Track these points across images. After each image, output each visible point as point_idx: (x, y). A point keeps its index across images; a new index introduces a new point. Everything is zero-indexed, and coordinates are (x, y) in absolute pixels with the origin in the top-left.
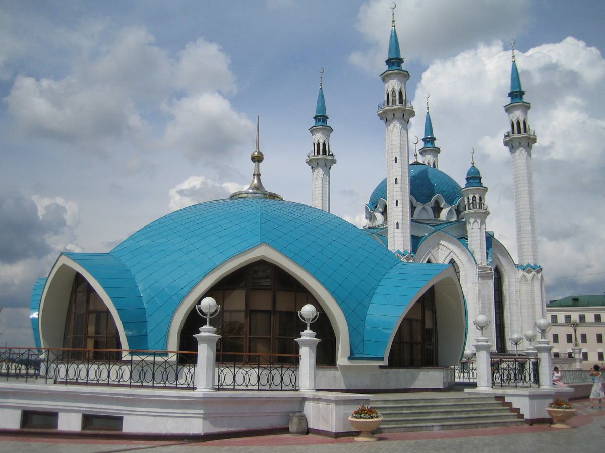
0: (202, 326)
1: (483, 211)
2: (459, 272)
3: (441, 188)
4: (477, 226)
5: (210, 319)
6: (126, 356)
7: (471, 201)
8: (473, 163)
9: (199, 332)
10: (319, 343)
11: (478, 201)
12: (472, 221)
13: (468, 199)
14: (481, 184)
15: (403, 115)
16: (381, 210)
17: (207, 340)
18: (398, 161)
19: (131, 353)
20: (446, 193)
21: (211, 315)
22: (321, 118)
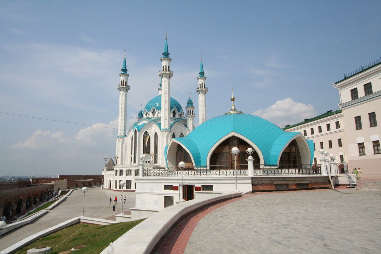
4: (191, 121)
5: (251, 154)
6: (261, 167)
11: (192, 112)
14: (192, 106)
16: (152, 112)
22: (125, 70)
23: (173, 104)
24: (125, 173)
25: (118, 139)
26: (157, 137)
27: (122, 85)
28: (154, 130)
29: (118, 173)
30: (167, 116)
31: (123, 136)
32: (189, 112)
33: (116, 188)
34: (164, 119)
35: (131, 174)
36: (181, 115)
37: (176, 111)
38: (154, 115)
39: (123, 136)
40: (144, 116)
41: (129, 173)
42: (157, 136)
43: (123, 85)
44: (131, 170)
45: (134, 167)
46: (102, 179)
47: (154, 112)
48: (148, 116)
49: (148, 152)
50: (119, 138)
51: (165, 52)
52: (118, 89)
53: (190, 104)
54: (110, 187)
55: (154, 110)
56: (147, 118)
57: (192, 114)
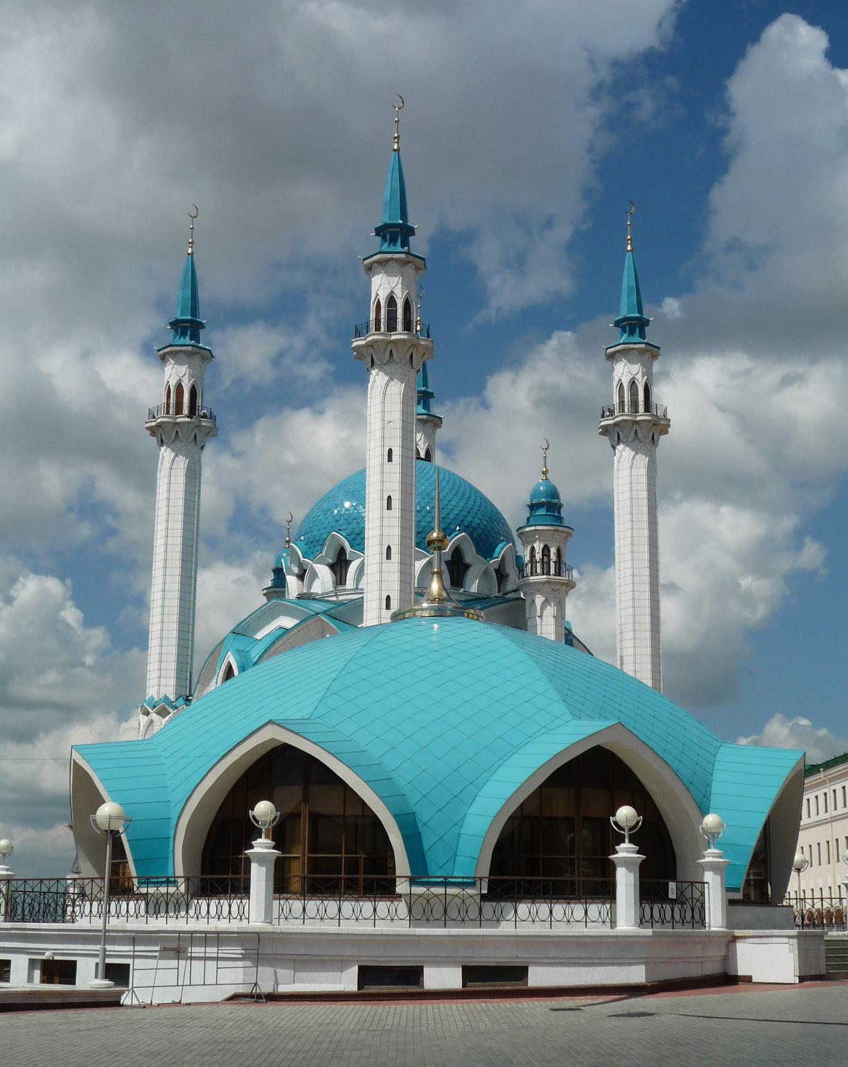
0: (620, 845)
1: (563, 578)
3: (469, 519)
6: (402, 887)
7: (538, 556)
8: (545, 473)
9: (616, 852)
10: (643, 861)
11: (553, 557)
12: (539, 600)
13: (533, 548)
14: (559, 519)
15: (411, 357)
17: (627, 863)
18: (394, 457)
19: (413, 881)
20: (479, 531)
21: (630, 830)
23: (452, 516)
27: (171, 410)
30: (396, 586)
31: (172, 698)
36: (501, 575)
37: (470, 555)
38: (340, 579)
39: (172, 698)
40: (291, 581)
43: (179, 410)
47: (339, 565)
48: (310, 587)
50: (147, 713)
51: (386, 219)
52: (153, 431)
53: (542, 512)
55: (342, 551)
56: (301, 597)
57: (558, 573)
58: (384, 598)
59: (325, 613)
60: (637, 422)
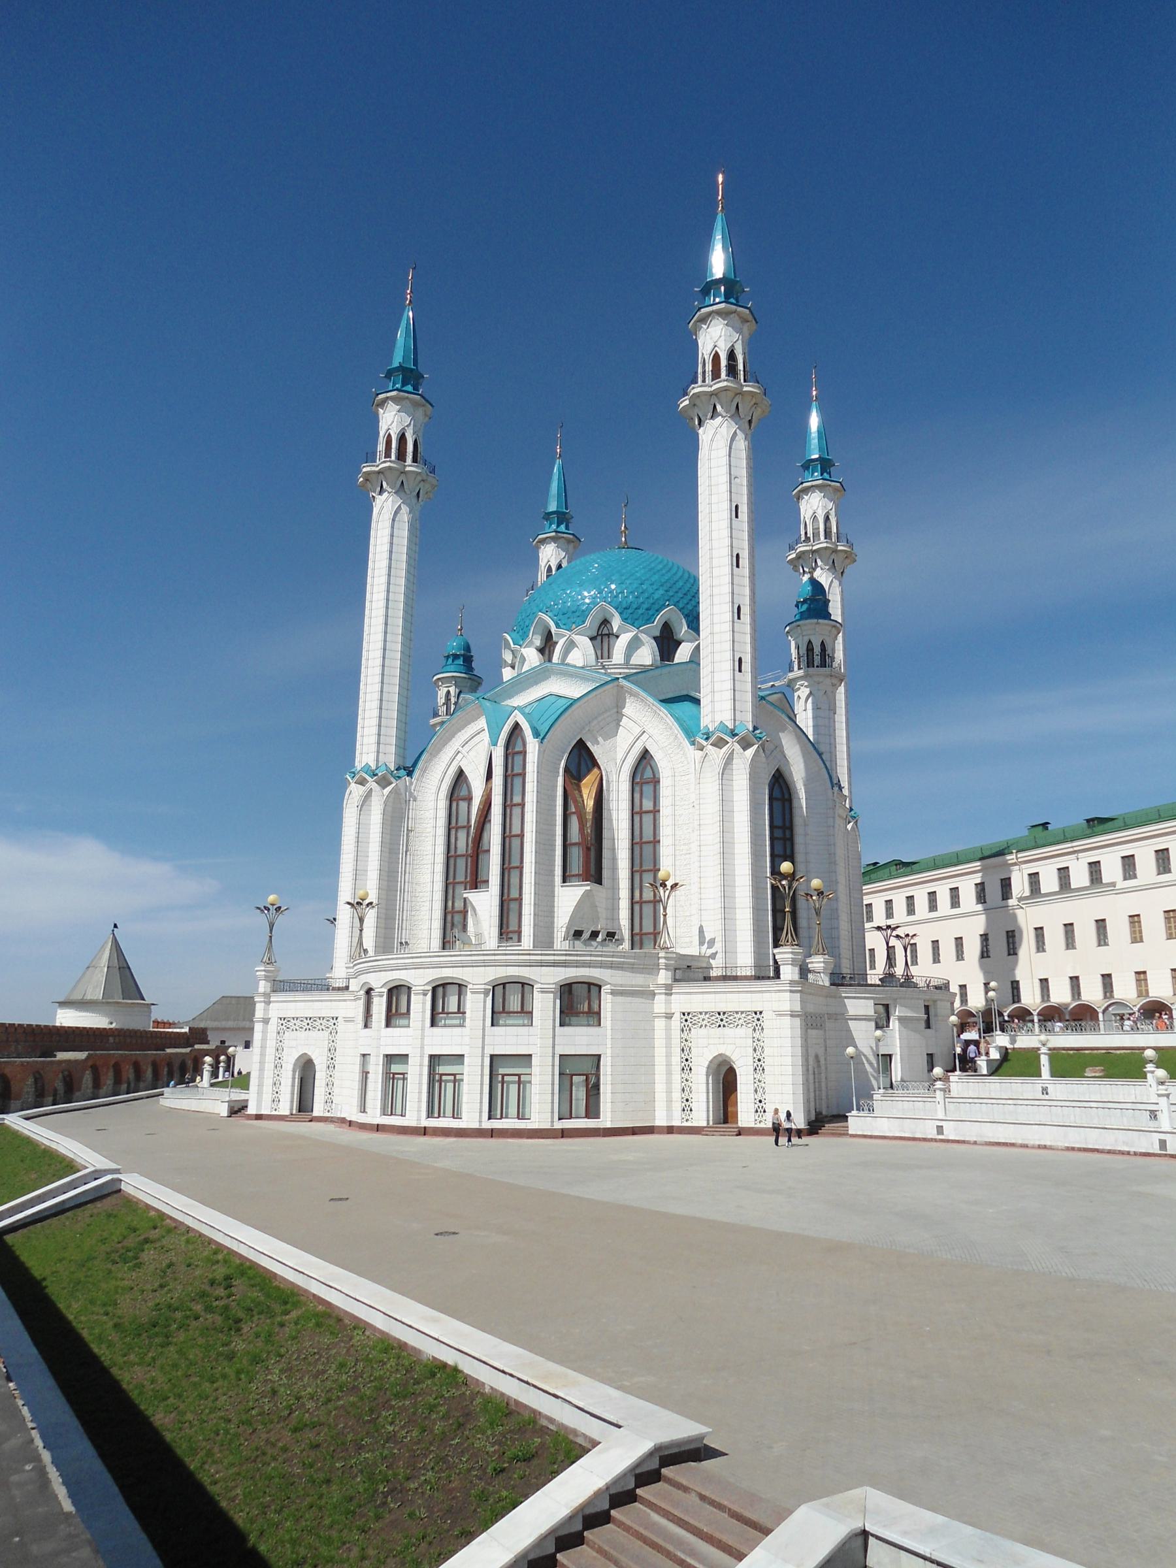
2: (790, 801)
7: (817, 650)
24: (477, 1006)
25: (355, 792)
26: (656, 782)
28: (631, 739)
29: (420, 1006)
32: (817, 650)
33: (389, 1107)
34: (728, 665)
35: (526, 1012)
41: (514, 1003)
42: (648, 774)
44: (525, 986)
45: (555, 964)
46: (850, 1050)
49: (593, 871)
50: (362, 782)
54: (304, 1104)
58: (737, 659)
59: (626, 677)
60: (835, 551)
